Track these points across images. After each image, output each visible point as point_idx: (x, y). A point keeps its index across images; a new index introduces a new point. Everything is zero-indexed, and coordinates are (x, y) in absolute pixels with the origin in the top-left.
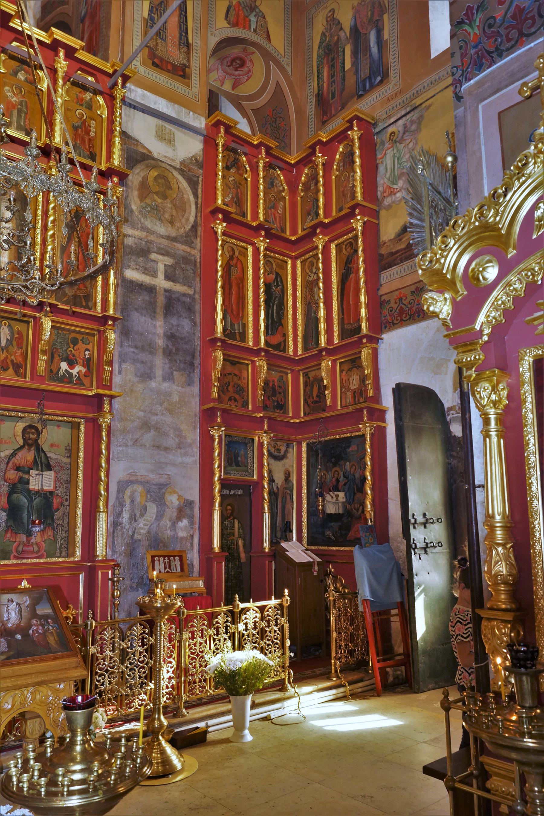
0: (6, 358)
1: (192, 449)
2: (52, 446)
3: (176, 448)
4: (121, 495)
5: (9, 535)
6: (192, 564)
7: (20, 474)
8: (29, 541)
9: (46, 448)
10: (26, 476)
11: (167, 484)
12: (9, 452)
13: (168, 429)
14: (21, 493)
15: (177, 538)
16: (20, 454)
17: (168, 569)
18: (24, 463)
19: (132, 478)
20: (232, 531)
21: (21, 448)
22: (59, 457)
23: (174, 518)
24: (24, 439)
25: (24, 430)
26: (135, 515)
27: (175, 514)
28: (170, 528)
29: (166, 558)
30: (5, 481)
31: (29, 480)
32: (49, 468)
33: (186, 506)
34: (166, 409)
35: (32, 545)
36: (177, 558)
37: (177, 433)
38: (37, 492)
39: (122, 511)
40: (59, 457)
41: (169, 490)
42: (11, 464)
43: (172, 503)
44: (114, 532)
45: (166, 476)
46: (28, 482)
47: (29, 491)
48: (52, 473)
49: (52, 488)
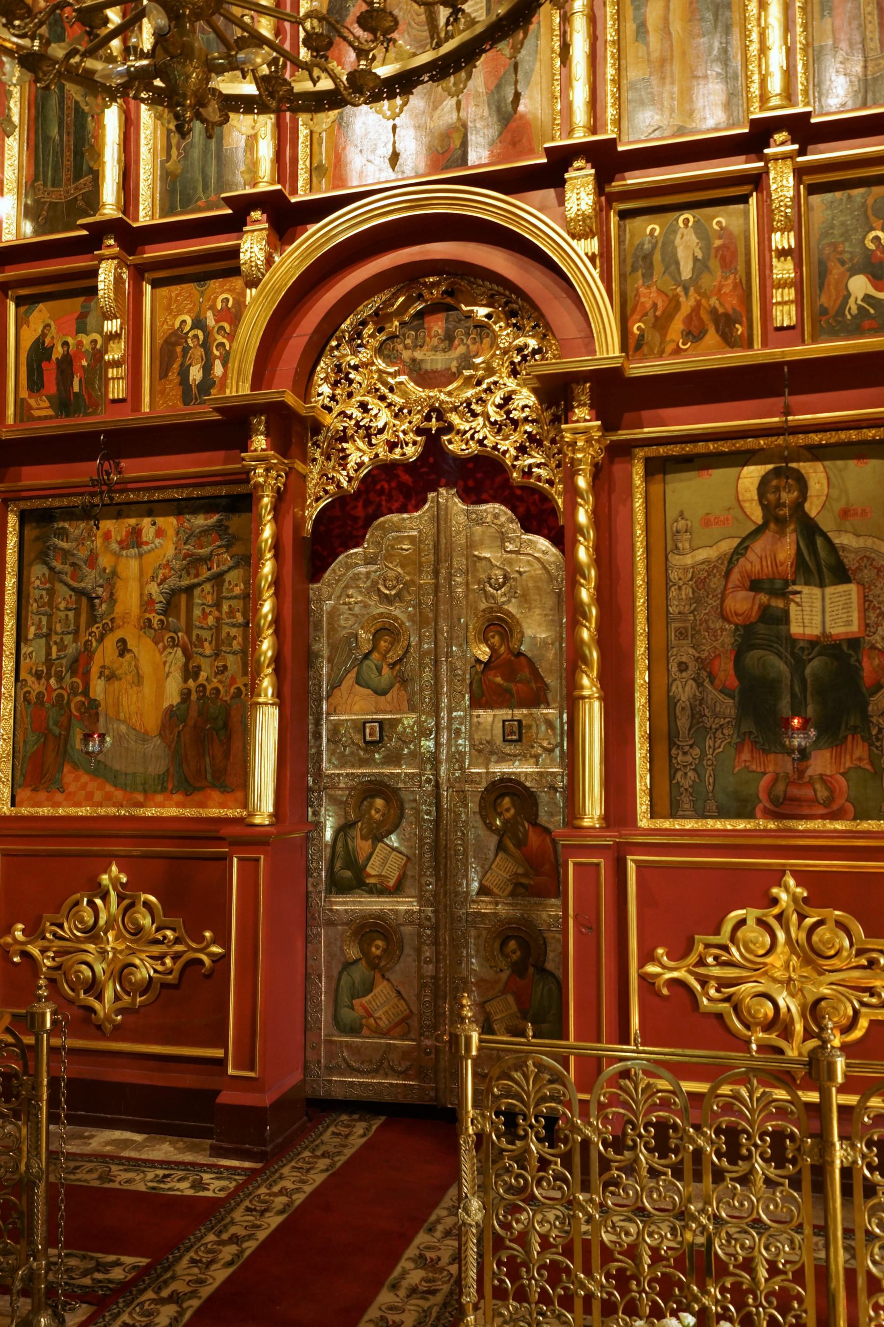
0: (697, 307)
2: (845, 513)
5: (746, 755)
7: (763, 598)
8: (801, 773)
9: (826, 524)
10: (779, 603)
12: (728, 546)
14: (768, 647)
16: (759, 546)
18: (768, 571)
21: (759, 531)
22: (869, 542)
24: (765, 508)
25: (764, 484)
30: (725, 618)
31: (787, 613)
32: (842, 575)
35: (811, 783)
38: (813, 643)
40: (869, 542)
42: (735, 576)
46: (784, 618)
47: (792, 641)
48: (853, 587)
49: (855, 628)
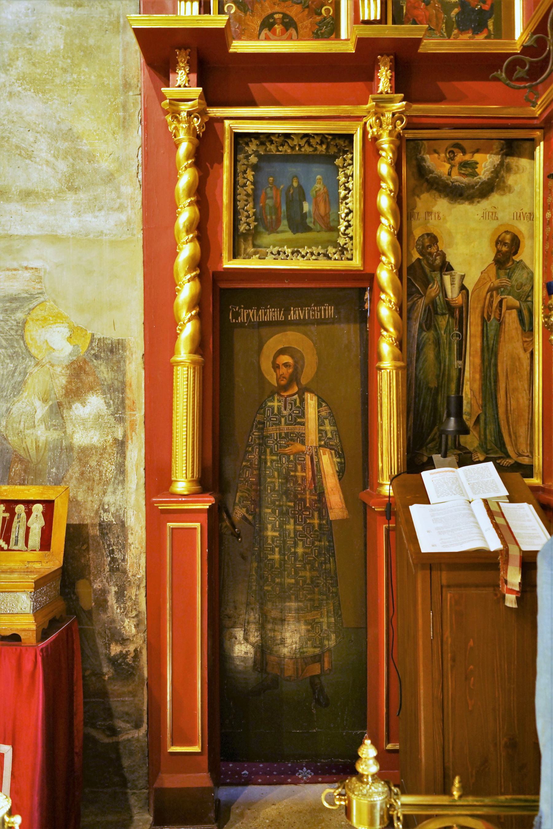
1: (117, 189)
3: (61, 191)
6: (123, 524)
11: (31, 297)
15: (70, 448)
20: (298, 429)
23: (59, 392)
27: (63, 381)
28: (43, 420)
33: (96, 357)
34: (22, 78)
36: (38, 509)
37: (64, 145)
41: (38, 313)
45: (27, 274)
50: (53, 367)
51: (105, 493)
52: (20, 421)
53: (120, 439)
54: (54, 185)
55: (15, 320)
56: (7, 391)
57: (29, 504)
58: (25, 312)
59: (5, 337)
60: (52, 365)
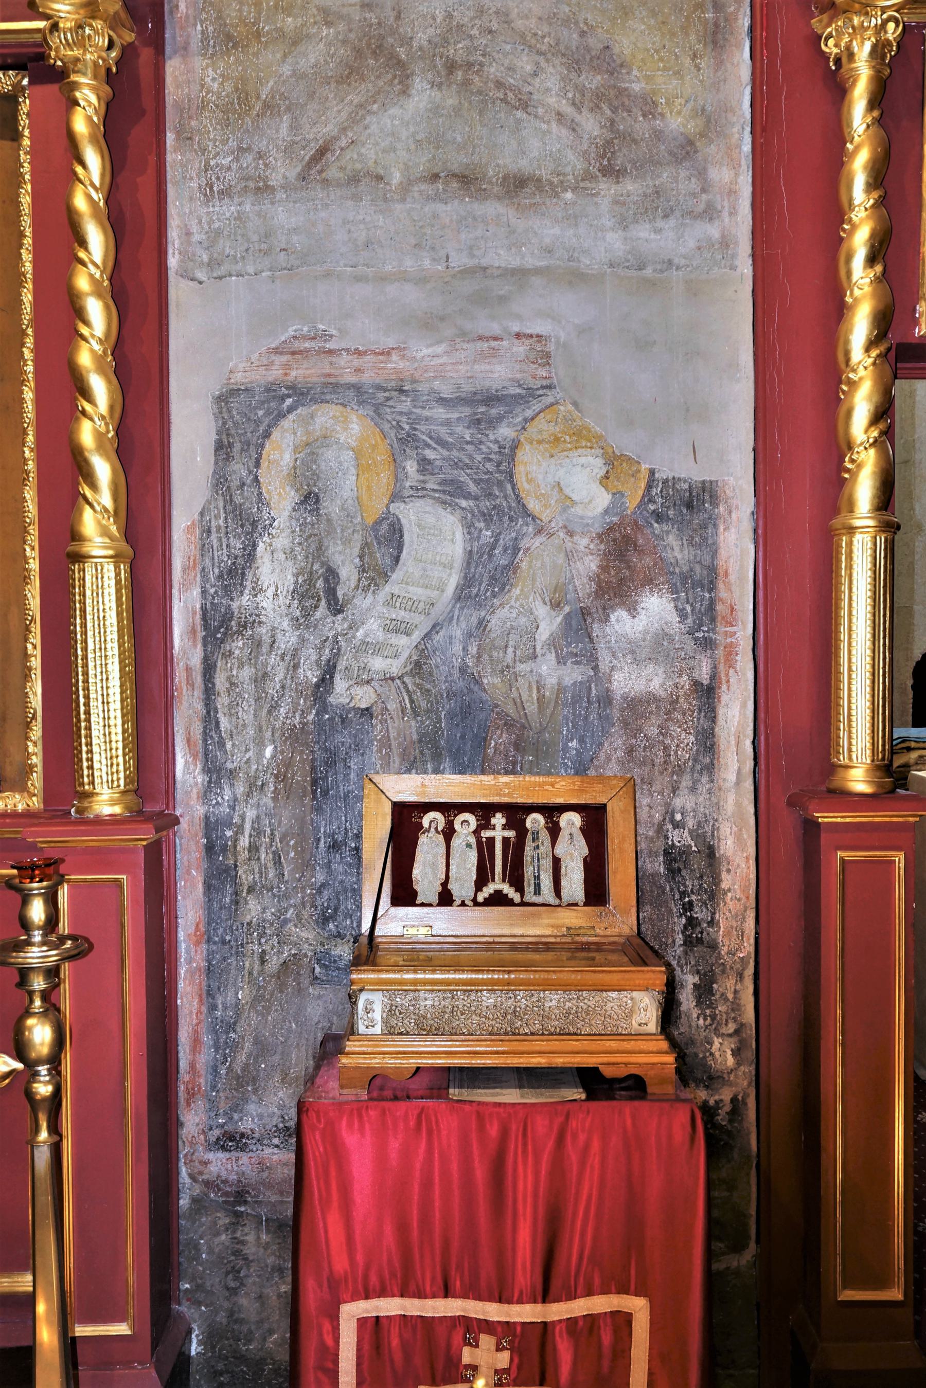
1: (702, 174)
3: (588, 176)
4: (239, 469)
6: (711, 853)
11: (531, 394)
13: (525, 64)
15: (606, 699)
17: (498, 885)
19: (302, 372)
26: (331, 575)
27: (592, 564)
28: (553, 643)
29: (499, 820)
33: (659, 517)
36: (571, 821)
37: (593, 81)
39: (250, 555)
43: (567, 502)
44: (209, 669)
45: (520, 349)
50: (571, 536)
51: (675, 790)
52: (506, 646)
53: (705, 682)
54: (574, 163)
55: (496, 441)
56: (480, 585)
57: (552, 811)
58: (515, 425)
59: (474, 476)
60: (571, 534)
